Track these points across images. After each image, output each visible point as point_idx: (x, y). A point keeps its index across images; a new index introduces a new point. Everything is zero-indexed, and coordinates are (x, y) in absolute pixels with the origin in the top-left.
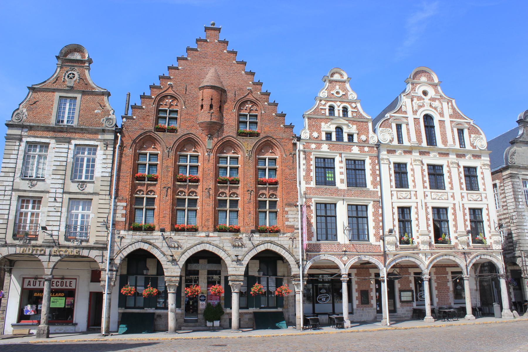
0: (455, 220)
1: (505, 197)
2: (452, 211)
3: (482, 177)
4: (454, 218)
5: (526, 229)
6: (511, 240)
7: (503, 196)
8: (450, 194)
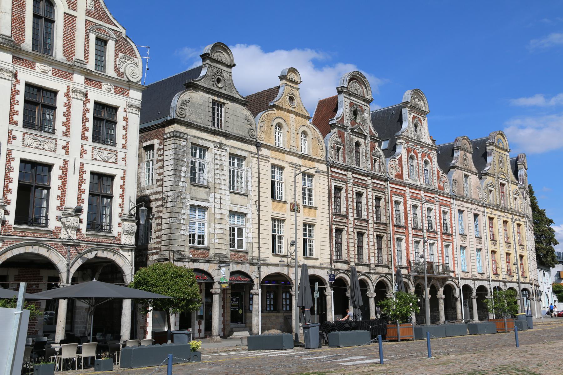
0: (63, 188)
1: (162, 167)
2: (60, 172)
3: (125, 125)
4: (60, 184)
5: (184, 219)
6: (160, 233)
7: (160, 164)
8: (61, 143)
